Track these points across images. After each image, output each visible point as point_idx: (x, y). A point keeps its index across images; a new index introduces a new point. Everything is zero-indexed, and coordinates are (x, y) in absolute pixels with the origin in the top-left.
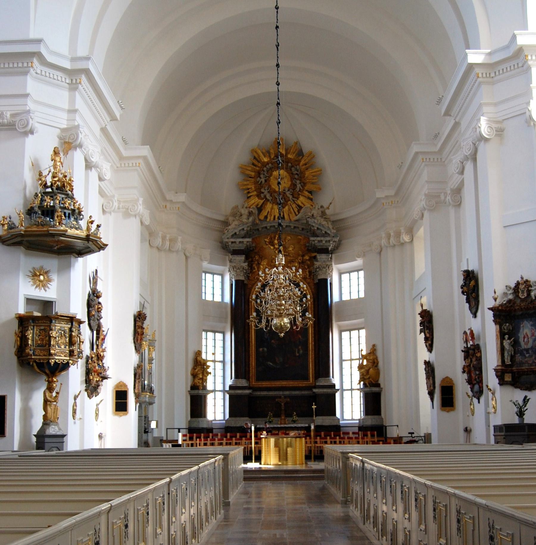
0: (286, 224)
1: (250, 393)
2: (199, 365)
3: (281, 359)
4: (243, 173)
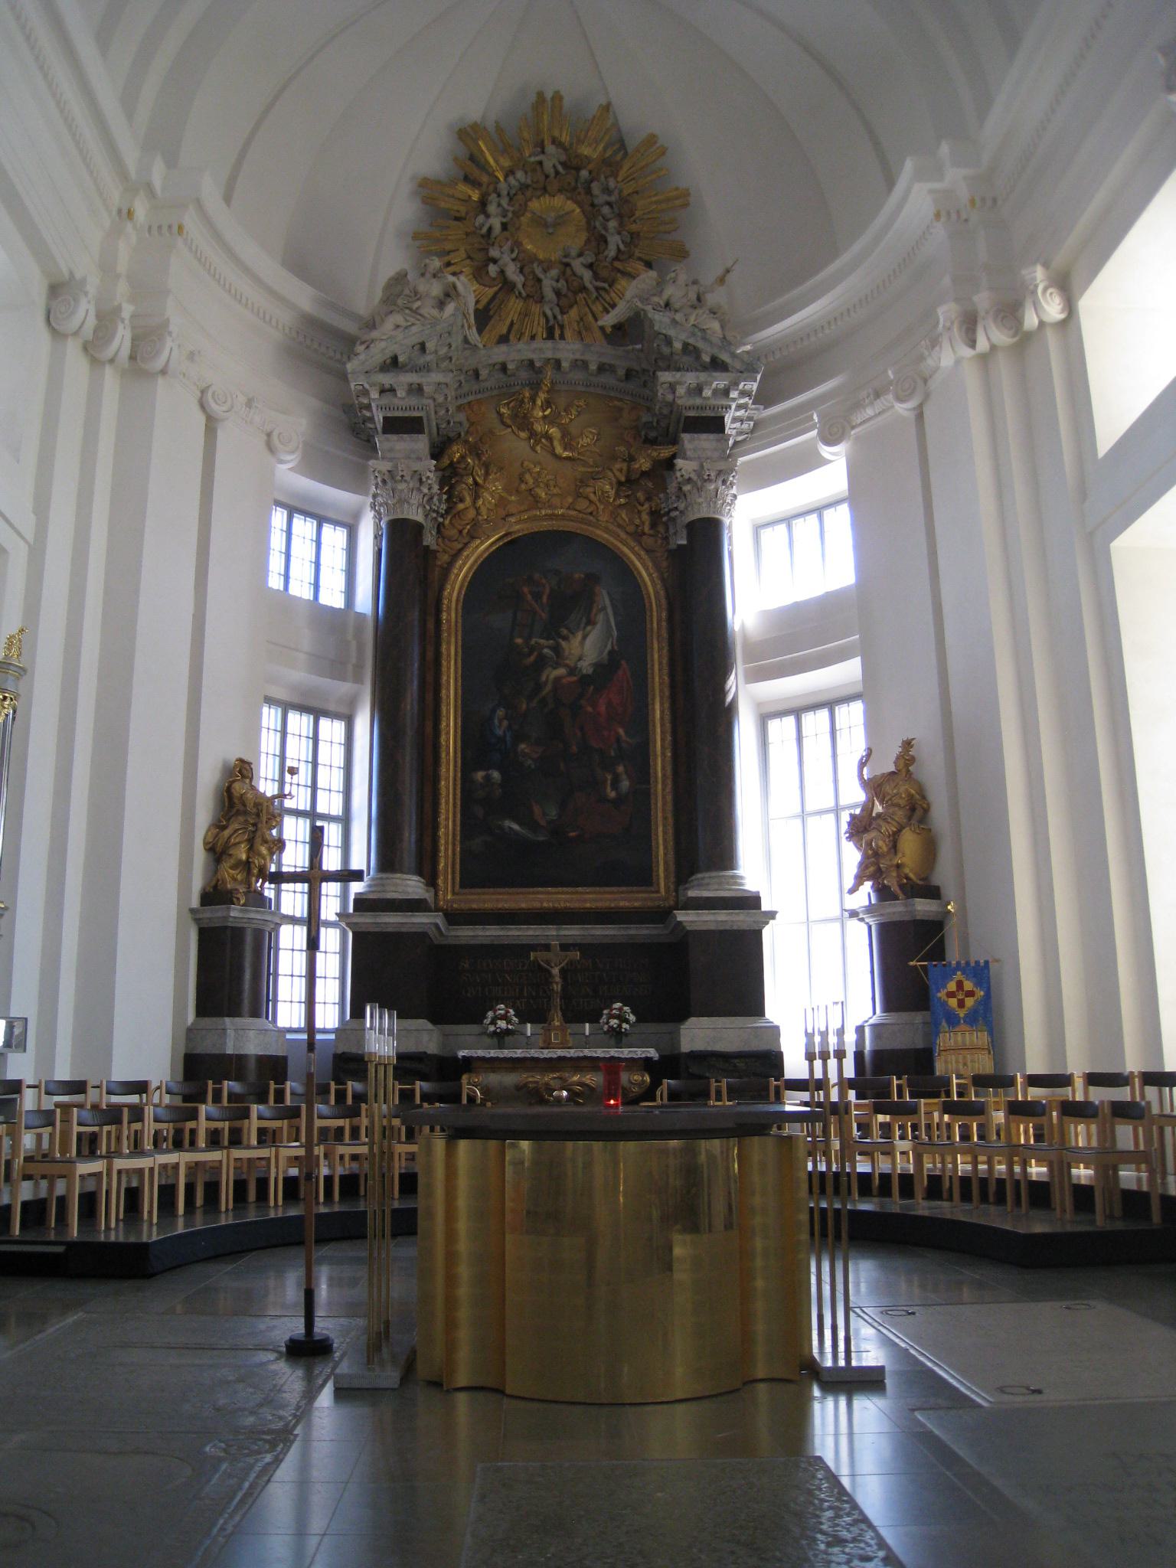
0: (572, 356)
1: (437, 926)
2: (238, 813)
3: (553, 813)
4: (429, 201)
